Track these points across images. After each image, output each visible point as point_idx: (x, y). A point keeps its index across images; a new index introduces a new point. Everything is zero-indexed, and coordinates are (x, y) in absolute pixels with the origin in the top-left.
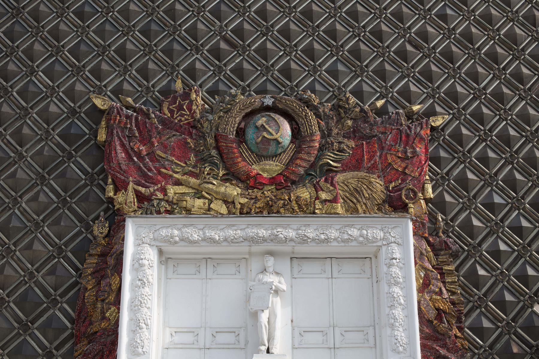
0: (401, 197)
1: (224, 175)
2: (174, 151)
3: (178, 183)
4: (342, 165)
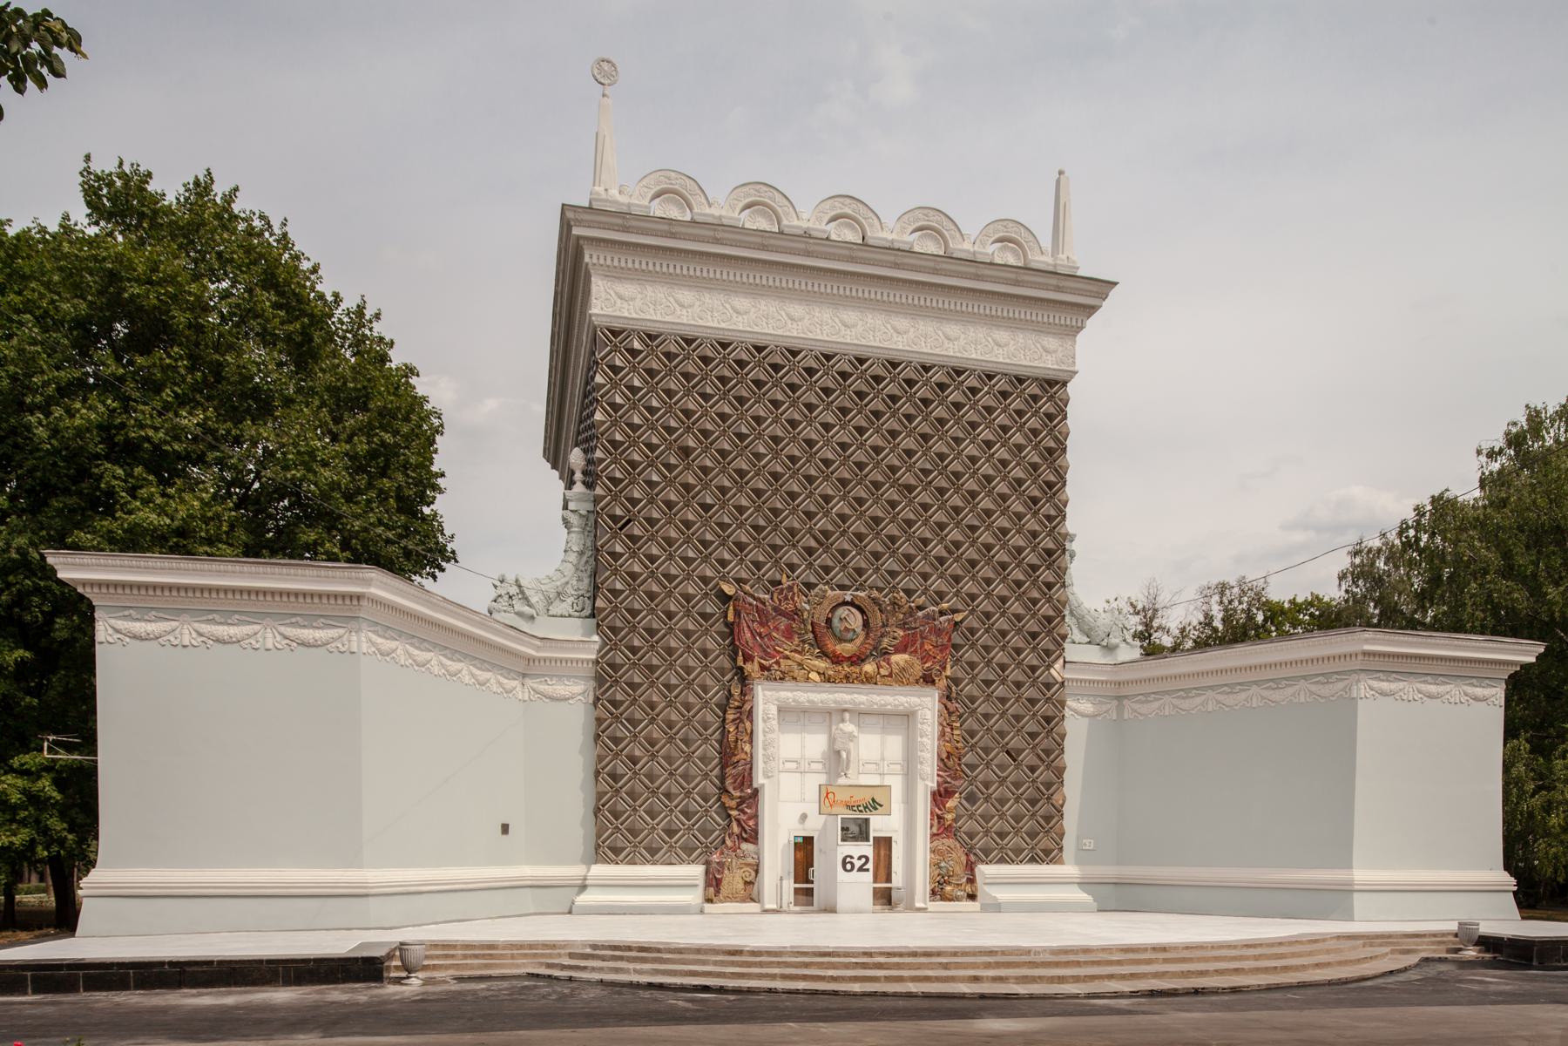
3: (787, 658)
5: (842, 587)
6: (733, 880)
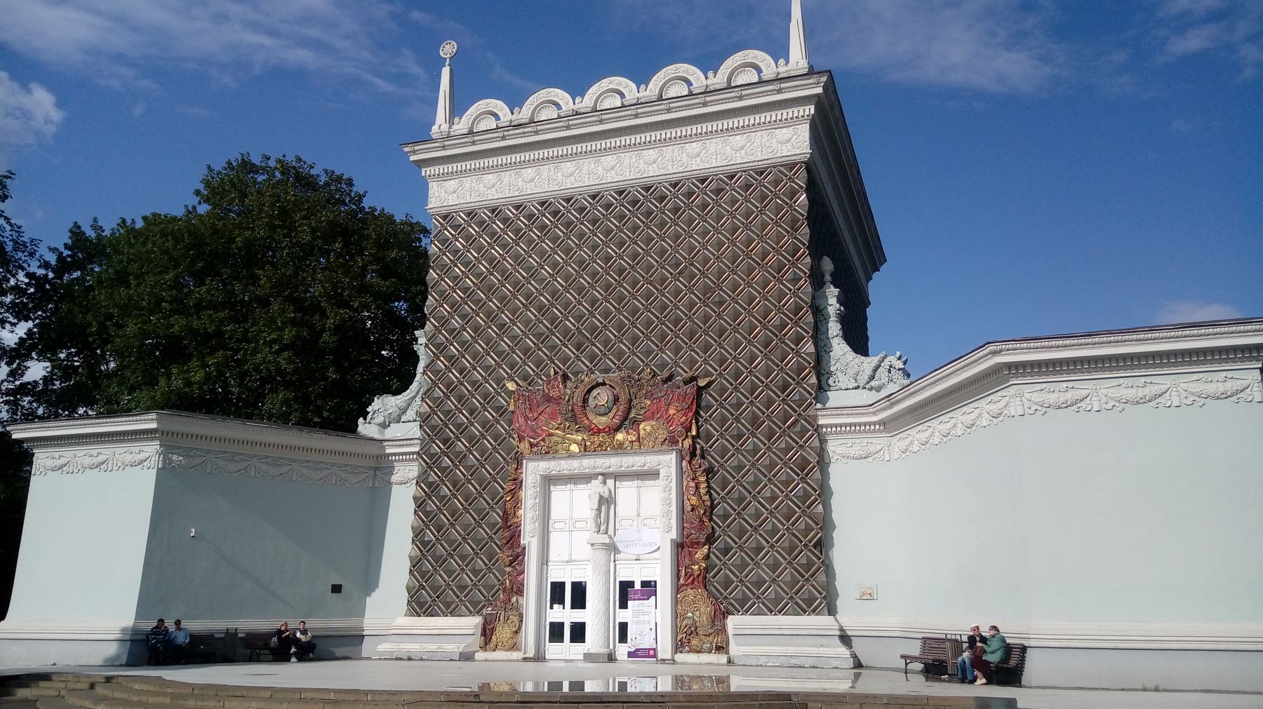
6: (503, 632)
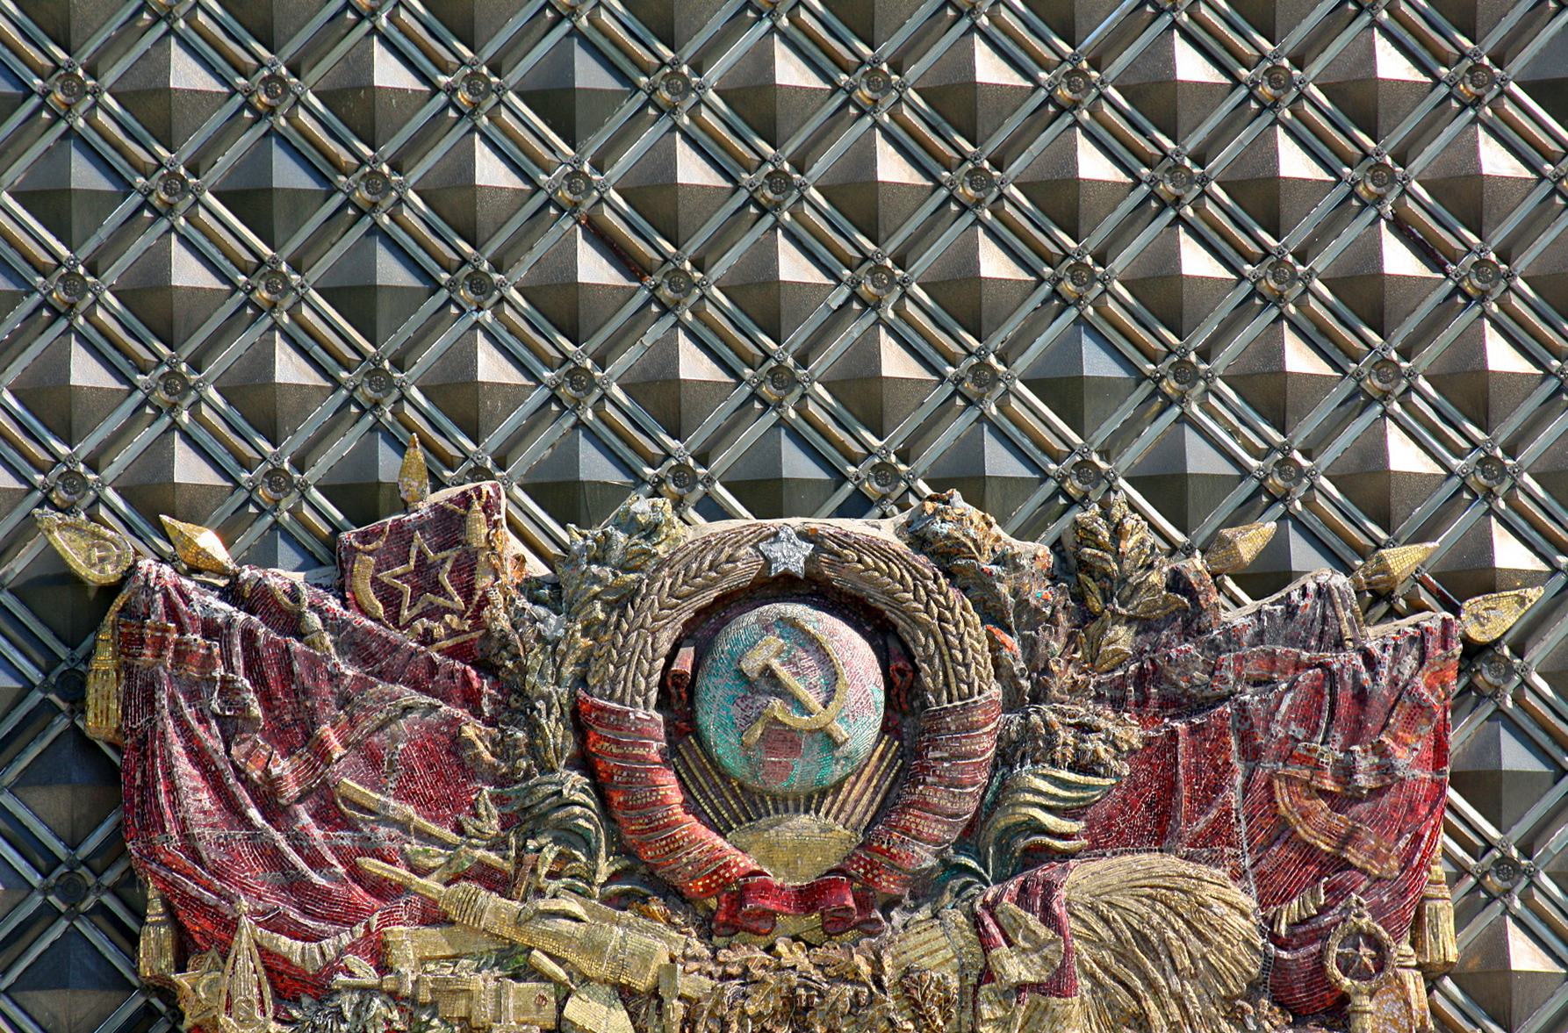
0: (1324, 968)
1: (613, 878)
2: (411, 778)
4: (1090, 827)
5: (765, 494)
